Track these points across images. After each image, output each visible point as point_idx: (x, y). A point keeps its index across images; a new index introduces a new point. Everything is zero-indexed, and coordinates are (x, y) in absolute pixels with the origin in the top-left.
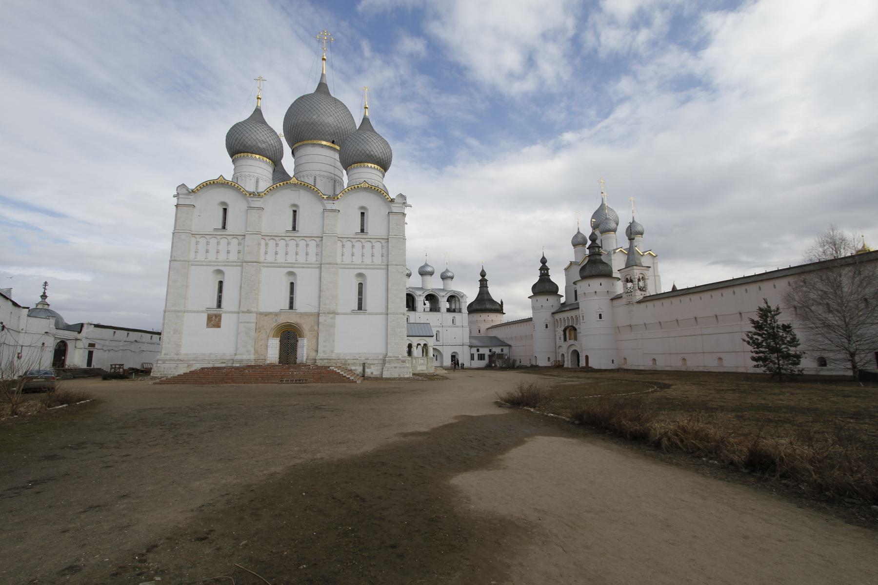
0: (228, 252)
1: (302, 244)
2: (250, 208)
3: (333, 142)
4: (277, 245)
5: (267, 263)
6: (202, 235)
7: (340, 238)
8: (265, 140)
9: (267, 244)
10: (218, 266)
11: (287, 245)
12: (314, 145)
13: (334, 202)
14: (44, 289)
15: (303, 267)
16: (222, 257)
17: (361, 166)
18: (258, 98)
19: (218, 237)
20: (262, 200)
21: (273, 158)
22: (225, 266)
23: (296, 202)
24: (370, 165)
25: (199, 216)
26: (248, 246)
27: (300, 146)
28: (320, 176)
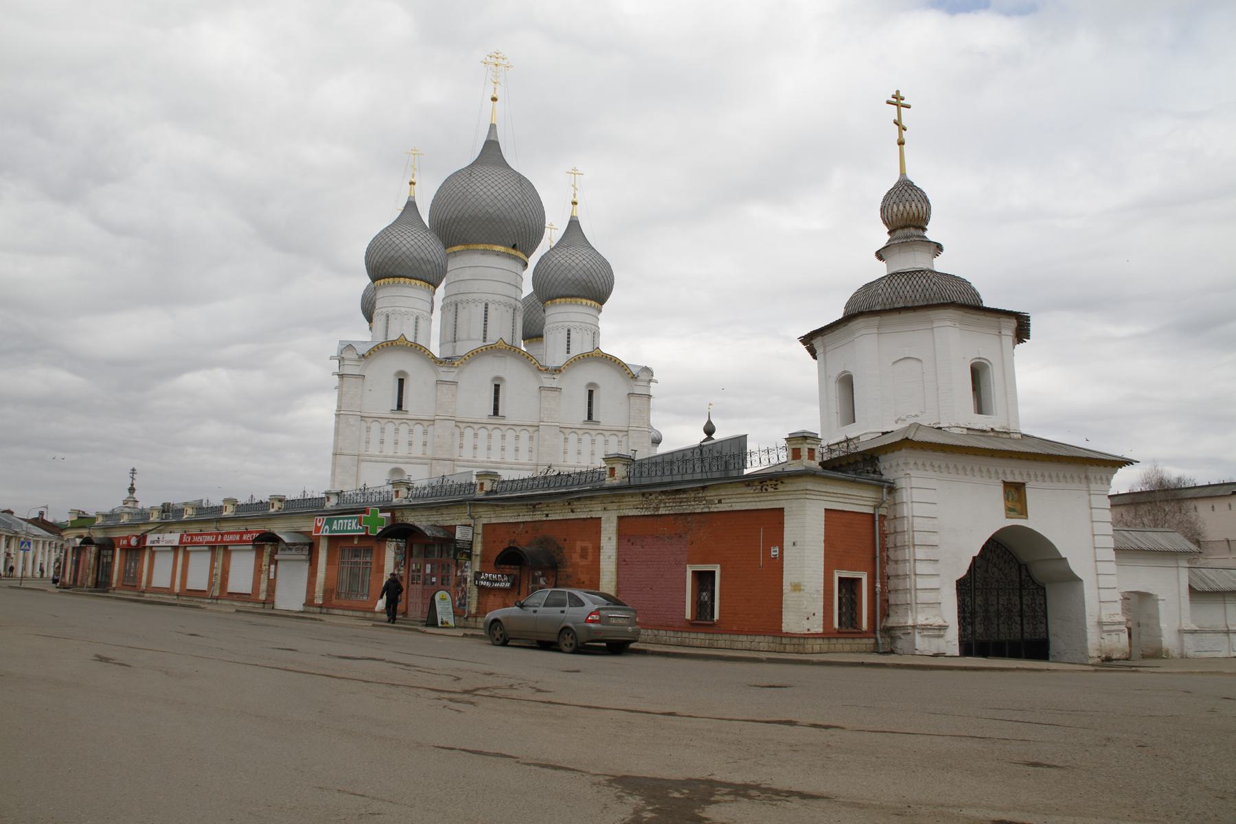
0: (410, 444)
1: (510, 435)
2: (440, 382)
3: (514, 247)
4: (476, 435)
5: (463, 461)
6: (374, 419)
7: (562, 429)
8: (431, 259)
9: (462, 434)
10: (396, 463)
11: (490, 436)
12: (485, 252)
13: (555, 376)
14: (131, 479)
15: (511, 469)
16: (403, 451)
17: (571, 303)
18: (412, 183)
19: (397, 422)
20: (456, 371)
21: (432, 279)
22: (407, 463)
23: (501, 374)
24: (584, 301)
25: (370, 390)
26: (438, 437)
27: (460, 252)
28: (494, 302)
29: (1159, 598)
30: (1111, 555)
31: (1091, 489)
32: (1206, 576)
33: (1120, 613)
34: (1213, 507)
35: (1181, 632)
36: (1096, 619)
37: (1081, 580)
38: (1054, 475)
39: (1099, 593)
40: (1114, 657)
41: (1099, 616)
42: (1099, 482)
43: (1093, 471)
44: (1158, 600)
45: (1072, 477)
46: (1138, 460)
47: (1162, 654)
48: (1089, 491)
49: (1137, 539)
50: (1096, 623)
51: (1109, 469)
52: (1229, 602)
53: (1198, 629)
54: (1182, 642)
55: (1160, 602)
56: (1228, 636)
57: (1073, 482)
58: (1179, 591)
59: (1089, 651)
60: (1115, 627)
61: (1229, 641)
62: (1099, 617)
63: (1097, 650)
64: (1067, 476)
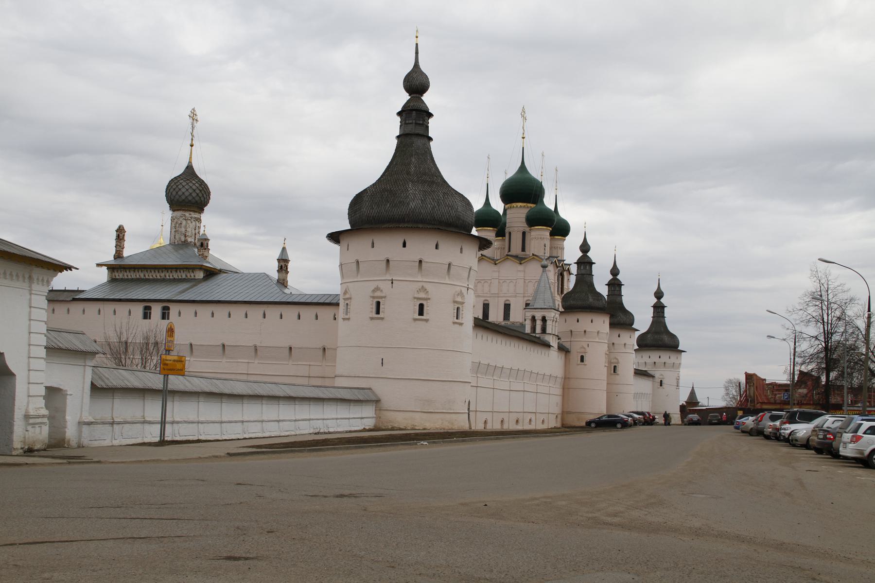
29: (68, 393)
30: (43, 353)
31: (33, 289)
32: (103, 375)
33: (44, 407)
34: (54, 310)
35: (81, 424)
36: (23, 413)
37: (14, 375)
38: (14, 274)
39: (28, 388)
40: (36, 448)
41: (26, 409)
42: (40, 283)
43: (37, 273)
44: (67, 395)
45: (17, 276)
46: (78, 268)
47: (65, 443)
48: (30, 290)
49: (55, 338)
50: (23, 417)
51: (51, 272)
52: (116, 397)
53: (94, 421)
54: (80, 432)
55: (68, 397)
56: (113, 427)
57: (18, 280)
58: (83, 388)
59: (14, 443)
60: (40, 420)
61: (113, 431)
62: (27, 411)
63: (21, 442)
64: (13, 273)
